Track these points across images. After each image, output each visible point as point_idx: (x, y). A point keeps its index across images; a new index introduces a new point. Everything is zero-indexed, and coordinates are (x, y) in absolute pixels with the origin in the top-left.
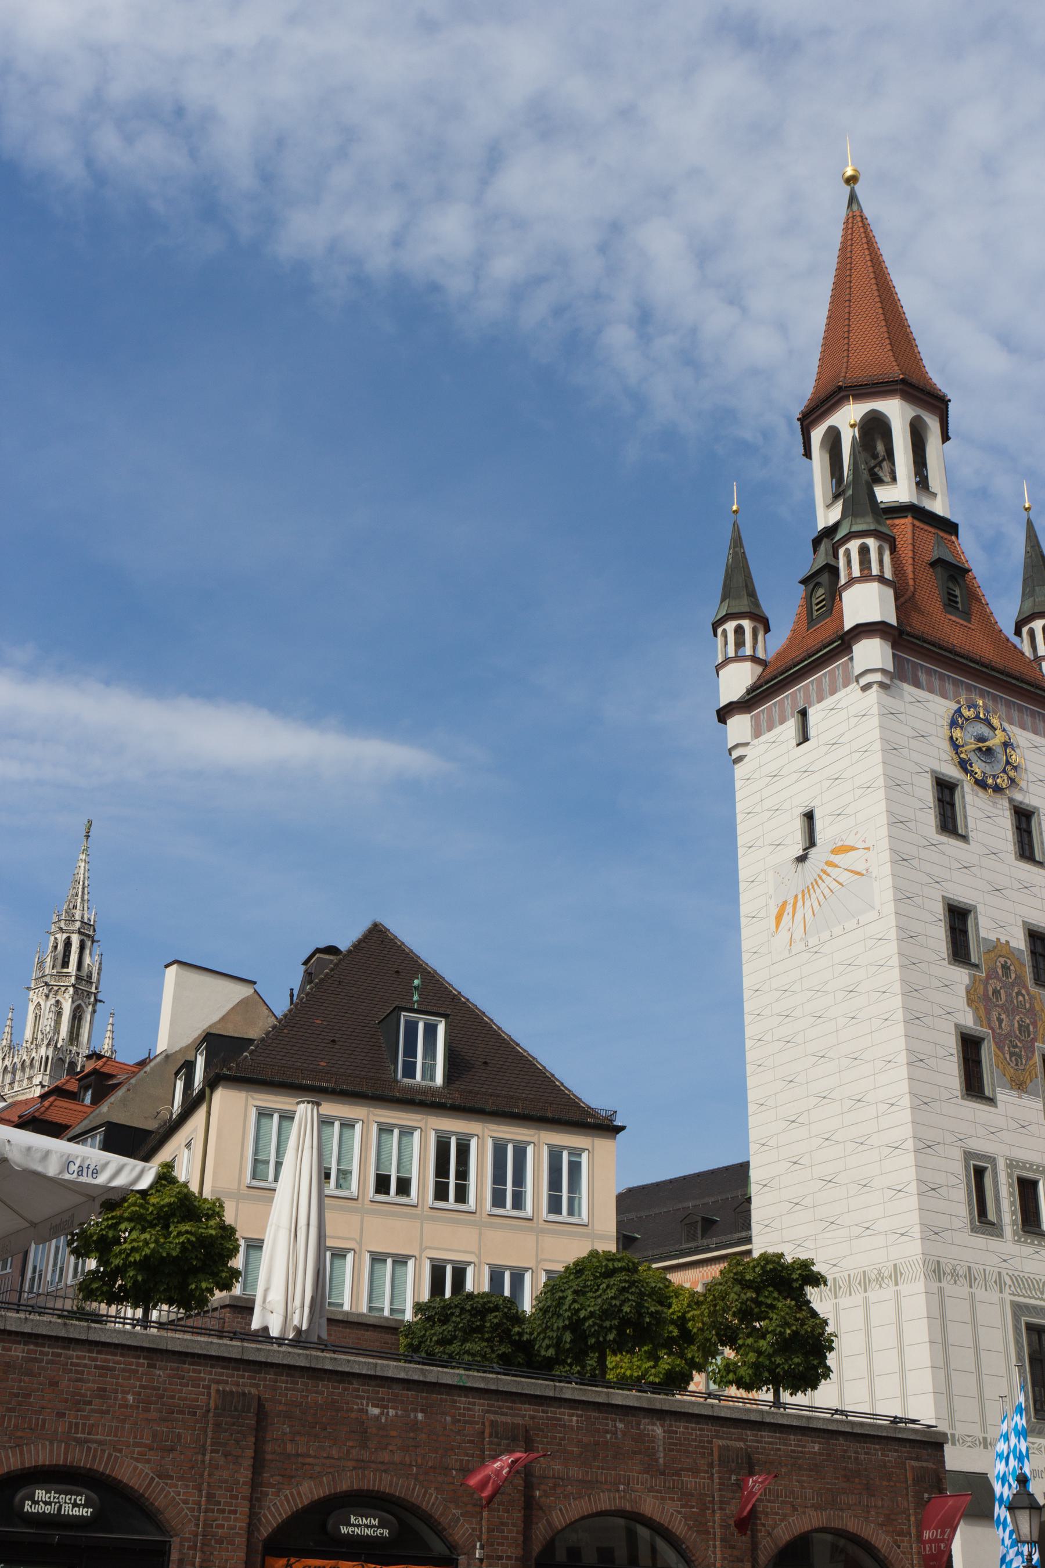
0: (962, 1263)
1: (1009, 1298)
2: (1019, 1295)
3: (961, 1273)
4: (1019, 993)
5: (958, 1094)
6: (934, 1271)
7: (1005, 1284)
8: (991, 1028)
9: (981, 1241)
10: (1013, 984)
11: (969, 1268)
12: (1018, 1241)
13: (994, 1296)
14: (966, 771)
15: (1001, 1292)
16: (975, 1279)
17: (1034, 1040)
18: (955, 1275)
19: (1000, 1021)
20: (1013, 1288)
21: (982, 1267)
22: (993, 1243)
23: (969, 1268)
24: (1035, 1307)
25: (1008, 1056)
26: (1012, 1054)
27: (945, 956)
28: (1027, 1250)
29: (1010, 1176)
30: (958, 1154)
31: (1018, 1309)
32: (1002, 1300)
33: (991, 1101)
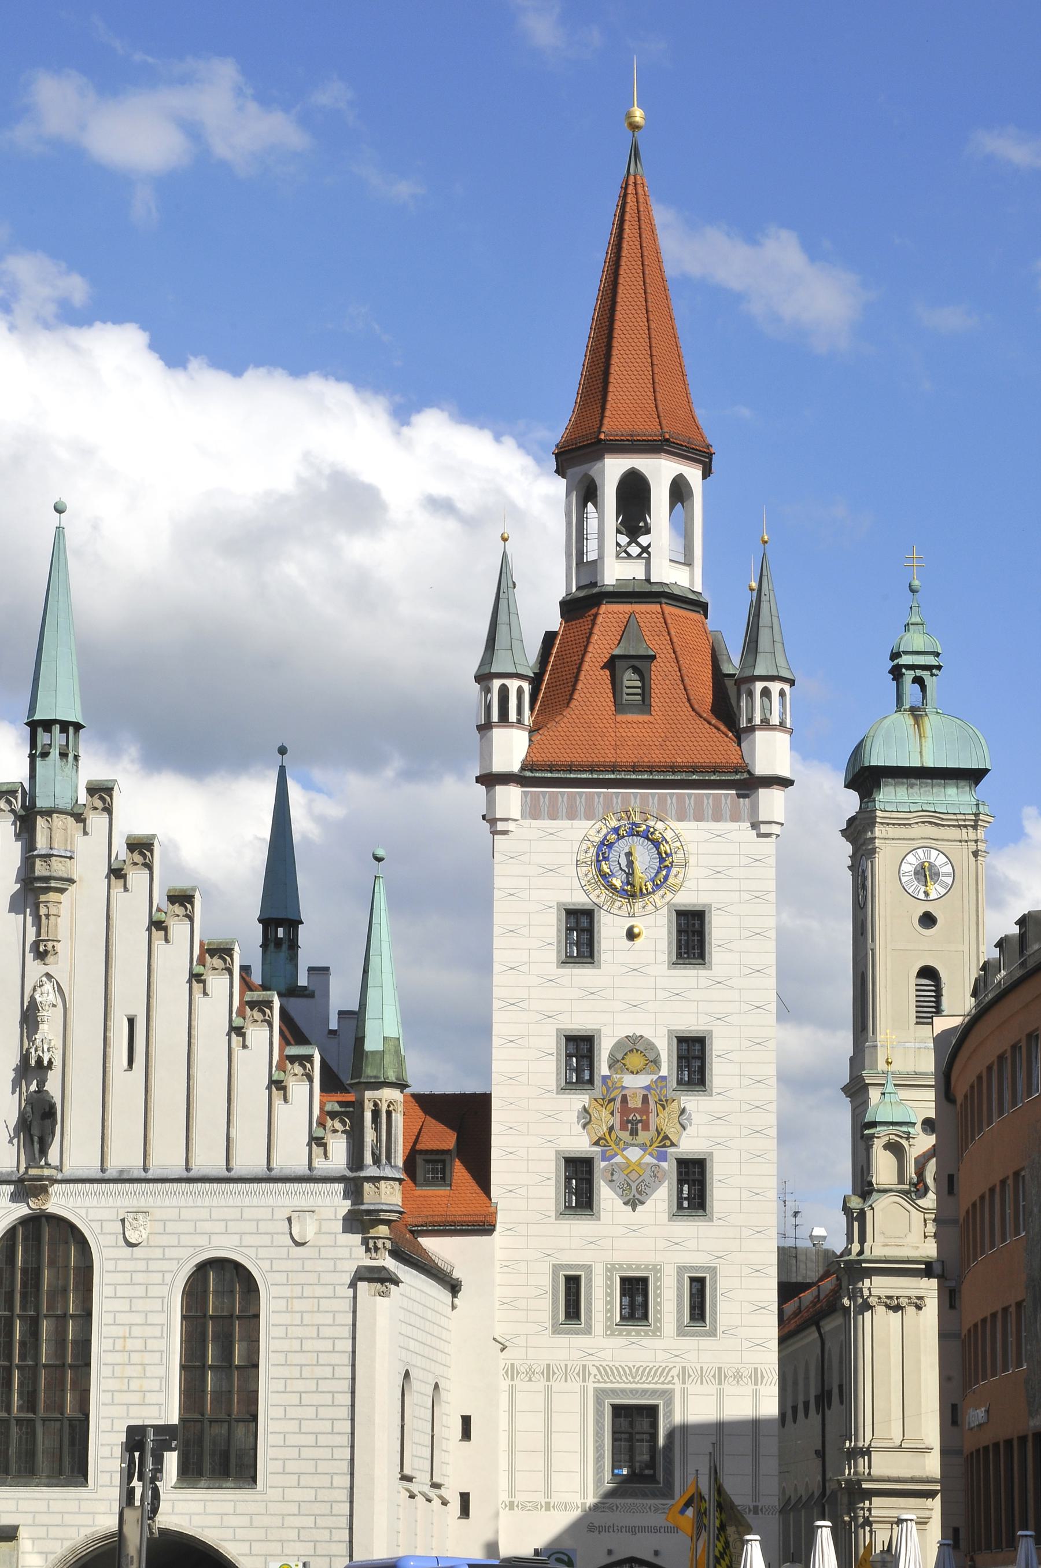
0: (540, 1362)
1: (591, 1386)
7: (590, 1374)
9: (563, 1340)
12: (612, 1334)
13: (575, 1385)
15: (584, 1381)
18: (530, 1373)
20: (599, 1377)
23: (548, 1365)
24: (623, 1391)
28: (621, 1341)
29: (609, 1278)
30: (546, 1268)
31: (600, 1395)
32: (584, 1389)
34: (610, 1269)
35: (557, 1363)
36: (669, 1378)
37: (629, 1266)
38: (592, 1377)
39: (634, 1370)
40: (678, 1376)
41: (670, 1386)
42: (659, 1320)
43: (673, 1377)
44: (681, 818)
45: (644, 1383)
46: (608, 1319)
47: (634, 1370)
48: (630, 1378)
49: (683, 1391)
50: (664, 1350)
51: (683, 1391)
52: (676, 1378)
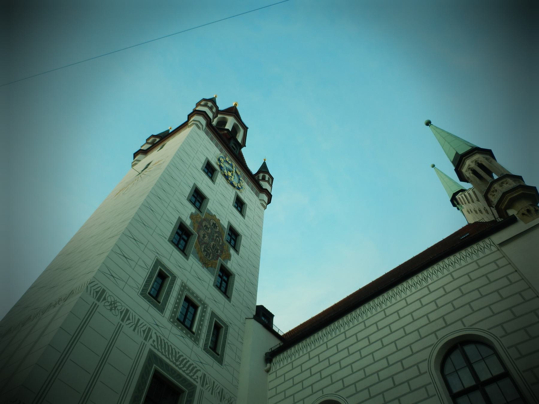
0: (123, 304)
1: (149, 345)
2: (158, 350)
3: (119, 308)
4: (217, 237)
5: (168, 238)
6: (97, 292)
7: (151, 337)
8: (198, 233)
10: (216, 232)
11: (127, 311)
12: (173, 322)
14: (221, 170)
15: (146, 339)
16: (129, 319)
17: (218, 256)
19: (204, 237)
20: (155, 343)
21: (137, 317)
22: (153, 311)
24: (167, 365)
25: (203, 249)
26: (204, 251)
27: (187, 197)
29: (181, 290)
32: (143, 346)
33: (186, 256)
34: (184, 287)
35: (134, 314)
36: (195, 377)
37: (193, 293)
38: (151, 341)
39: (178, 356)
40: (201, 378)
41: (195, 383)
42: (199, 335)
43: (197, 377)
44: (244, 179)
45: (180, 369)
46: (173, 312)
47: (178, 356)
48: (174, 359)
49: (201, 392)
50: (196, 354)
51: (201, 392)
52: (199, 380)
